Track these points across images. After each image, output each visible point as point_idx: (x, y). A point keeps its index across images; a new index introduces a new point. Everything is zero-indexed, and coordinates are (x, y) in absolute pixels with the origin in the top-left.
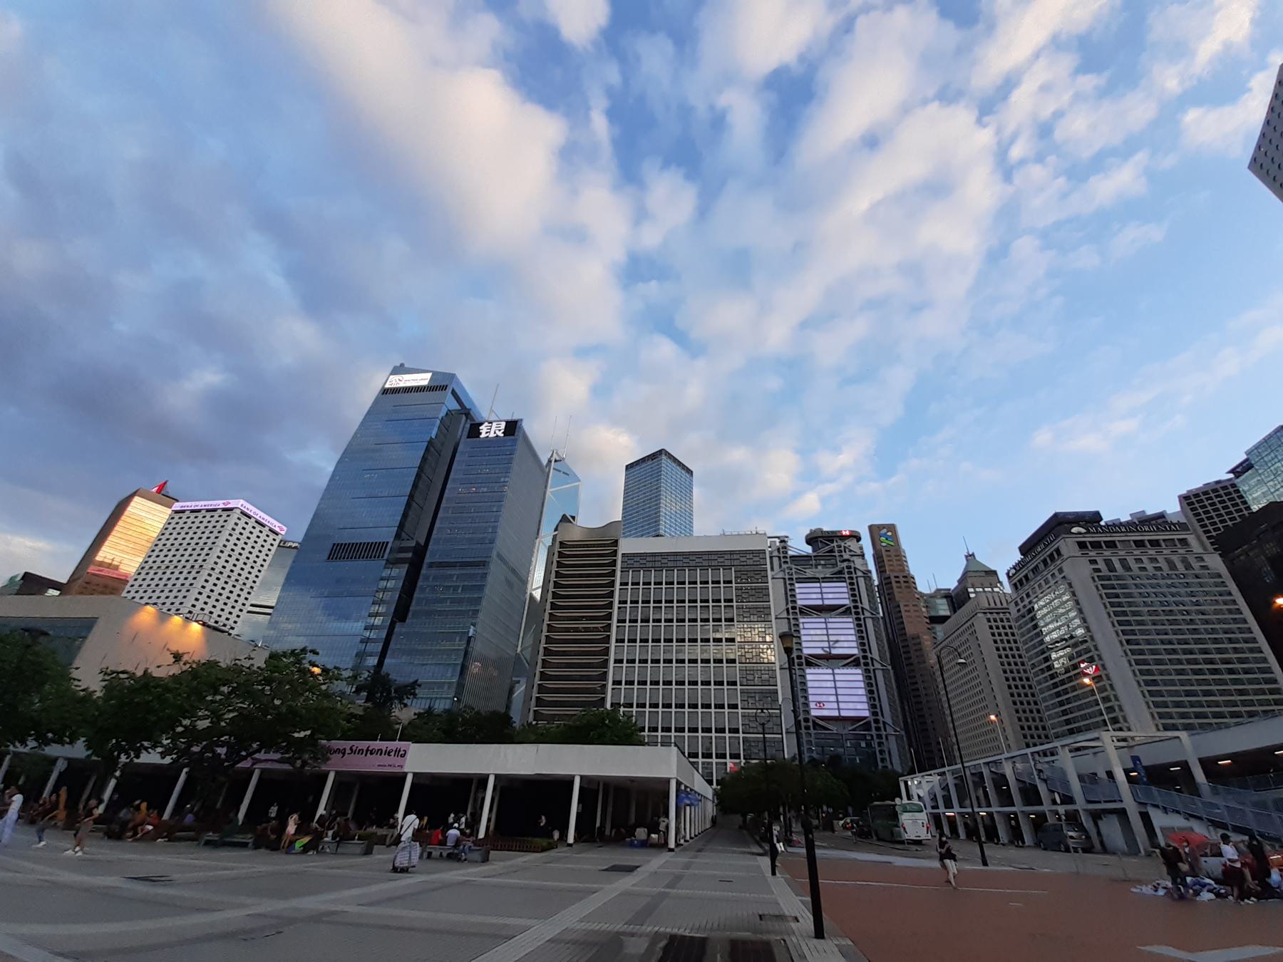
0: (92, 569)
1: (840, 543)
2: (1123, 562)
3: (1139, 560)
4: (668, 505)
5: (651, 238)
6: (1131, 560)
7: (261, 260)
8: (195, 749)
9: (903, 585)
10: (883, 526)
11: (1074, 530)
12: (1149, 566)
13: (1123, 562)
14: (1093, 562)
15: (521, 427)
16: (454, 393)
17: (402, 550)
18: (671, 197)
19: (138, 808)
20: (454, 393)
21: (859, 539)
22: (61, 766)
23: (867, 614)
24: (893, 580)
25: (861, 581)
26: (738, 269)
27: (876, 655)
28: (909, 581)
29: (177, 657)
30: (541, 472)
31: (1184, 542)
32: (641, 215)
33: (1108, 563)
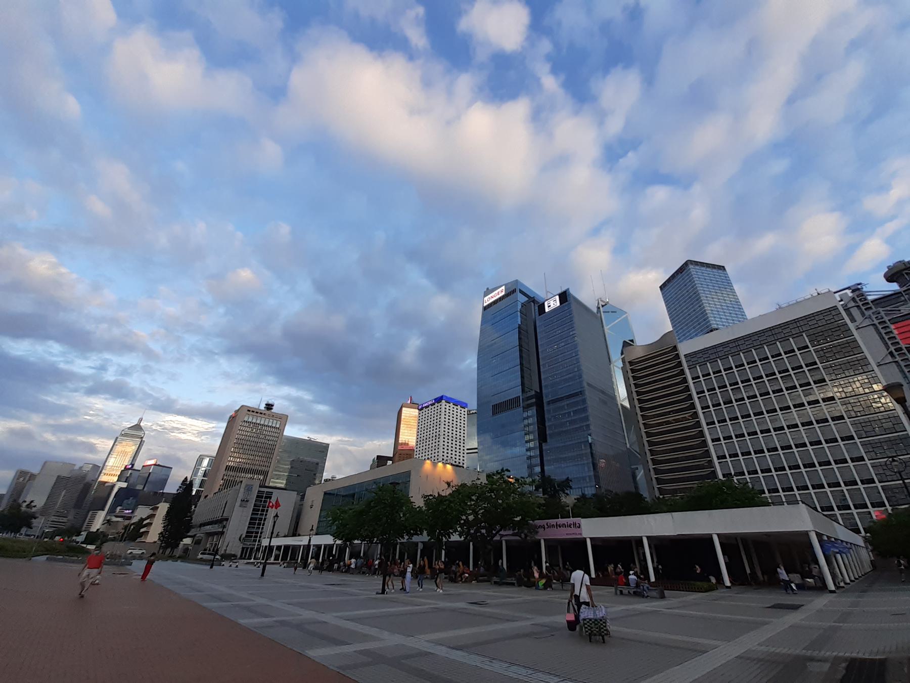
0: (400, 448)
4: (711, 304)
5: (615, 126)
7: (415, 275)
8: (472, 531)
15: (570, 294)
16: (521, 292)
17: (529, 398)
18: (621, 92)
19: (458, 564)
20: (521, 292)
22: (420, 546)
26: (700, 100)
29: (448, 484)
30: (596, 317)
32: (601, 117)
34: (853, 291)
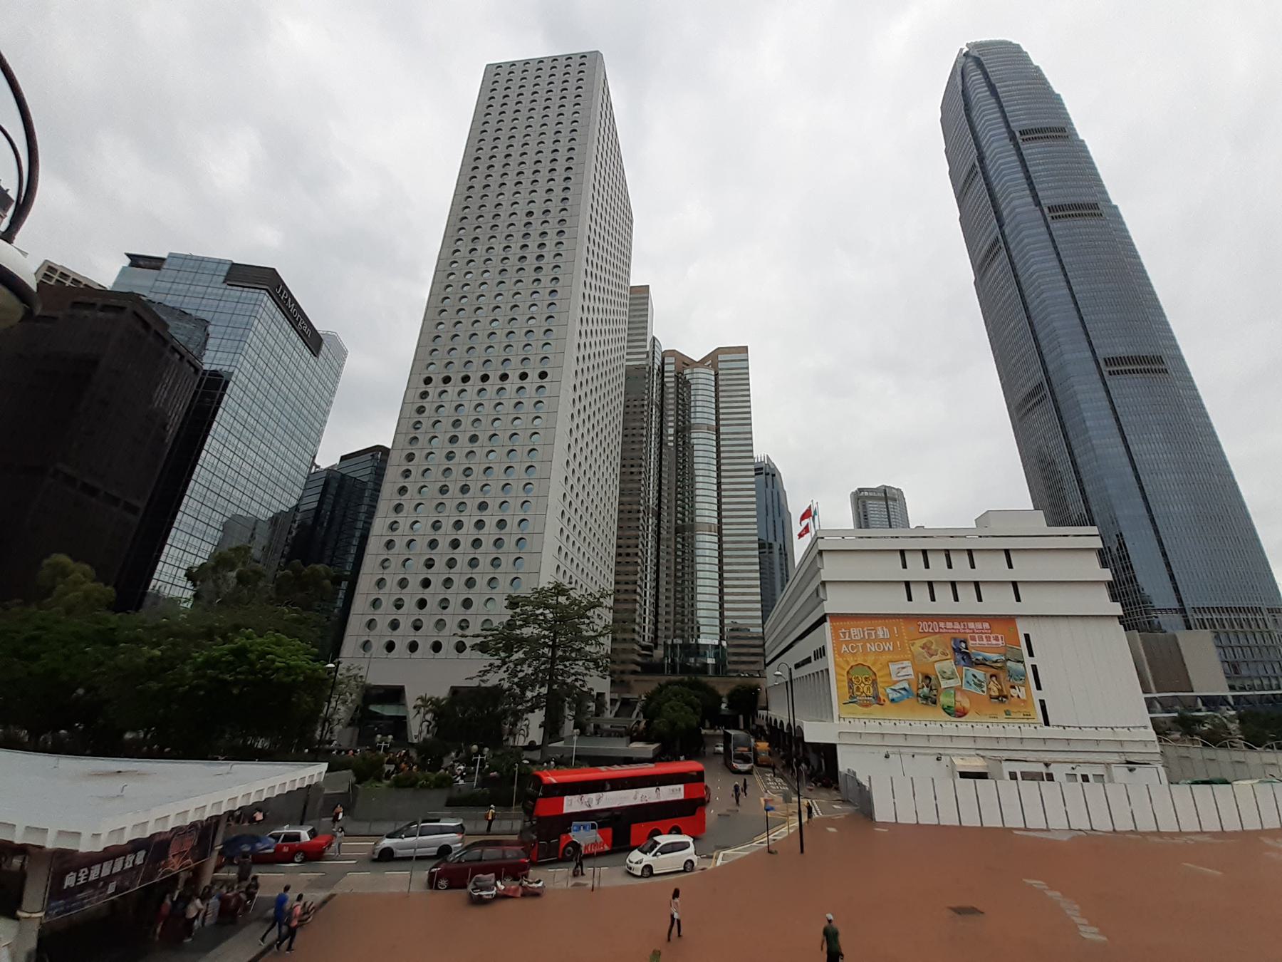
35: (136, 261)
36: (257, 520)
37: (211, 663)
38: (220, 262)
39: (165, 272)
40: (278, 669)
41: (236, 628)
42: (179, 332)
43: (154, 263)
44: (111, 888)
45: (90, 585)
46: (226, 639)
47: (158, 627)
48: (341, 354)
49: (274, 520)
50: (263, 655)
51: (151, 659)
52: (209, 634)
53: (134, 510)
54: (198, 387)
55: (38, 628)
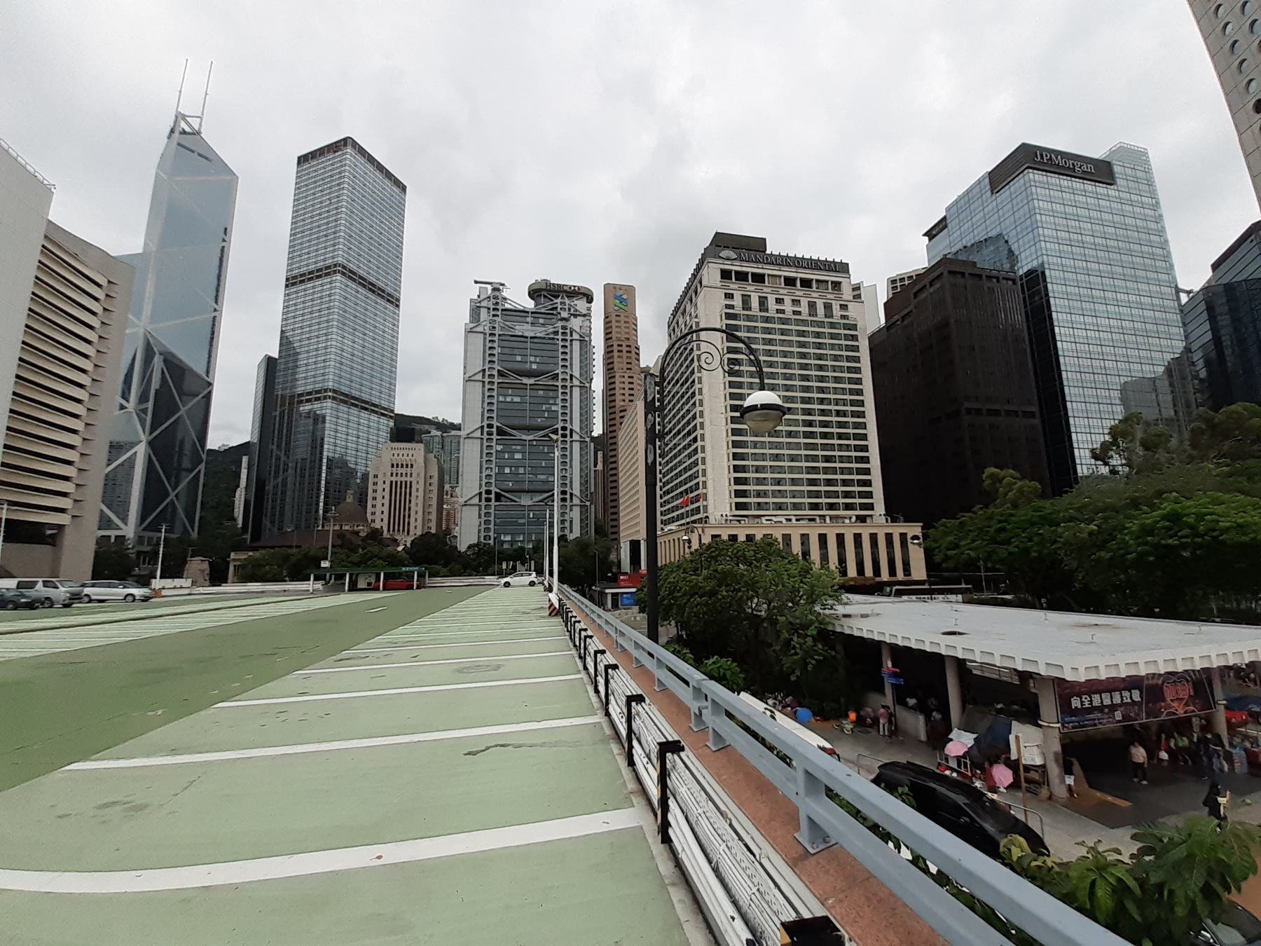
1: (567, 300)
2: (763, 302)
3: (779, 301)
6: (771, 299)
9: (625, 354)
10: (621, 287)
11: (724, 253)
12: (788, 307)
13: (763, 302)
14: (729, 296)
21: (590, 300)
23: (576, 382)
24: (615, 348)
25: (576, 345)
27: (576, 428)
28: (633, 351)
31: (837, 285)
33: (746, 300)
34: (495, 289)
35: (930, 234)
36: (1154, 380)
37: (1147, 531)
38: (979, 182)
39: (952, 225)
40: (1227, 530)
41: (1159, 494)
42: (985, 260)
43: (941, 225)
44: (1118, 715)
45: (1020, 483)
46: (1153, 507)
47: (1085, 506)
48: (1139, 159)
49: (1169, 371)
50: (1200, 517)
51: (1091, 534)
52: (1135, 504)
53: (1032, 415)
54: (1023, 292)
55: (1000, 522)
